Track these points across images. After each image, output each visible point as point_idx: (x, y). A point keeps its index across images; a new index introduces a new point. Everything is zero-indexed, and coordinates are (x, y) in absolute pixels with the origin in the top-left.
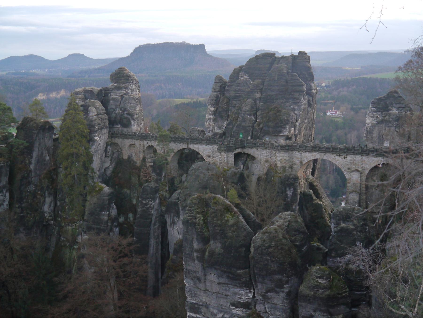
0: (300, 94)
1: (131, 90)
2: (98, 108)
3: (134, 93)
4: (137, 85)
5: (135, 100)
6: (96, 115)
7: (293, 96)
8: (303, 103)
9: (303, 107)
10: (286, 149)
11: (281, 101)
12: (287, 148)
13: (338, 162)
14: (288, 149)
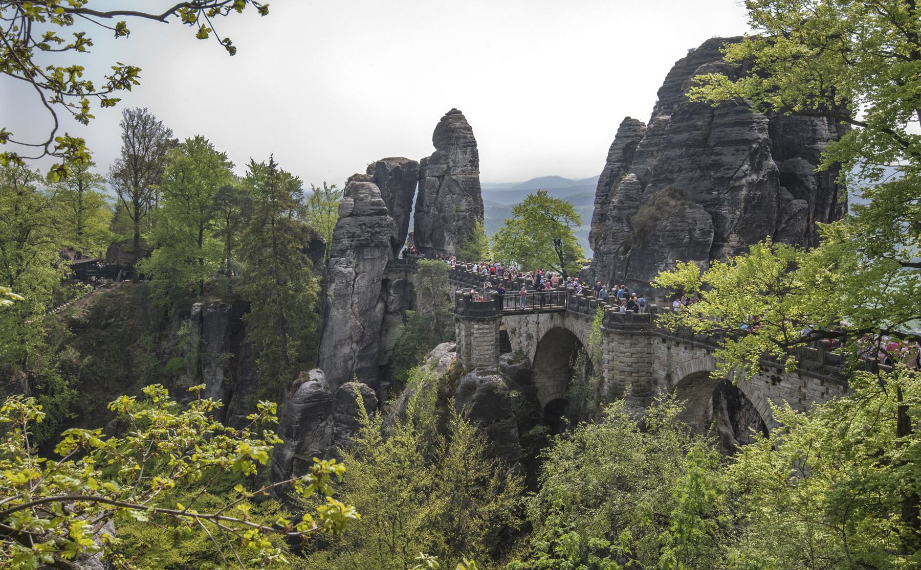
0: (737, 150)
1: (454, 161)
2: (362, 199)
3: (459, 170)
4: (469, 149)
5: (458, 185)
6: (351, 215)
7: (717, 158)
8: (744, 181)
9: (744, 192)
10: (623, 328)
11: (691, 174)
12: (627, 323)
13: (756, 393)
14: (633, 328)
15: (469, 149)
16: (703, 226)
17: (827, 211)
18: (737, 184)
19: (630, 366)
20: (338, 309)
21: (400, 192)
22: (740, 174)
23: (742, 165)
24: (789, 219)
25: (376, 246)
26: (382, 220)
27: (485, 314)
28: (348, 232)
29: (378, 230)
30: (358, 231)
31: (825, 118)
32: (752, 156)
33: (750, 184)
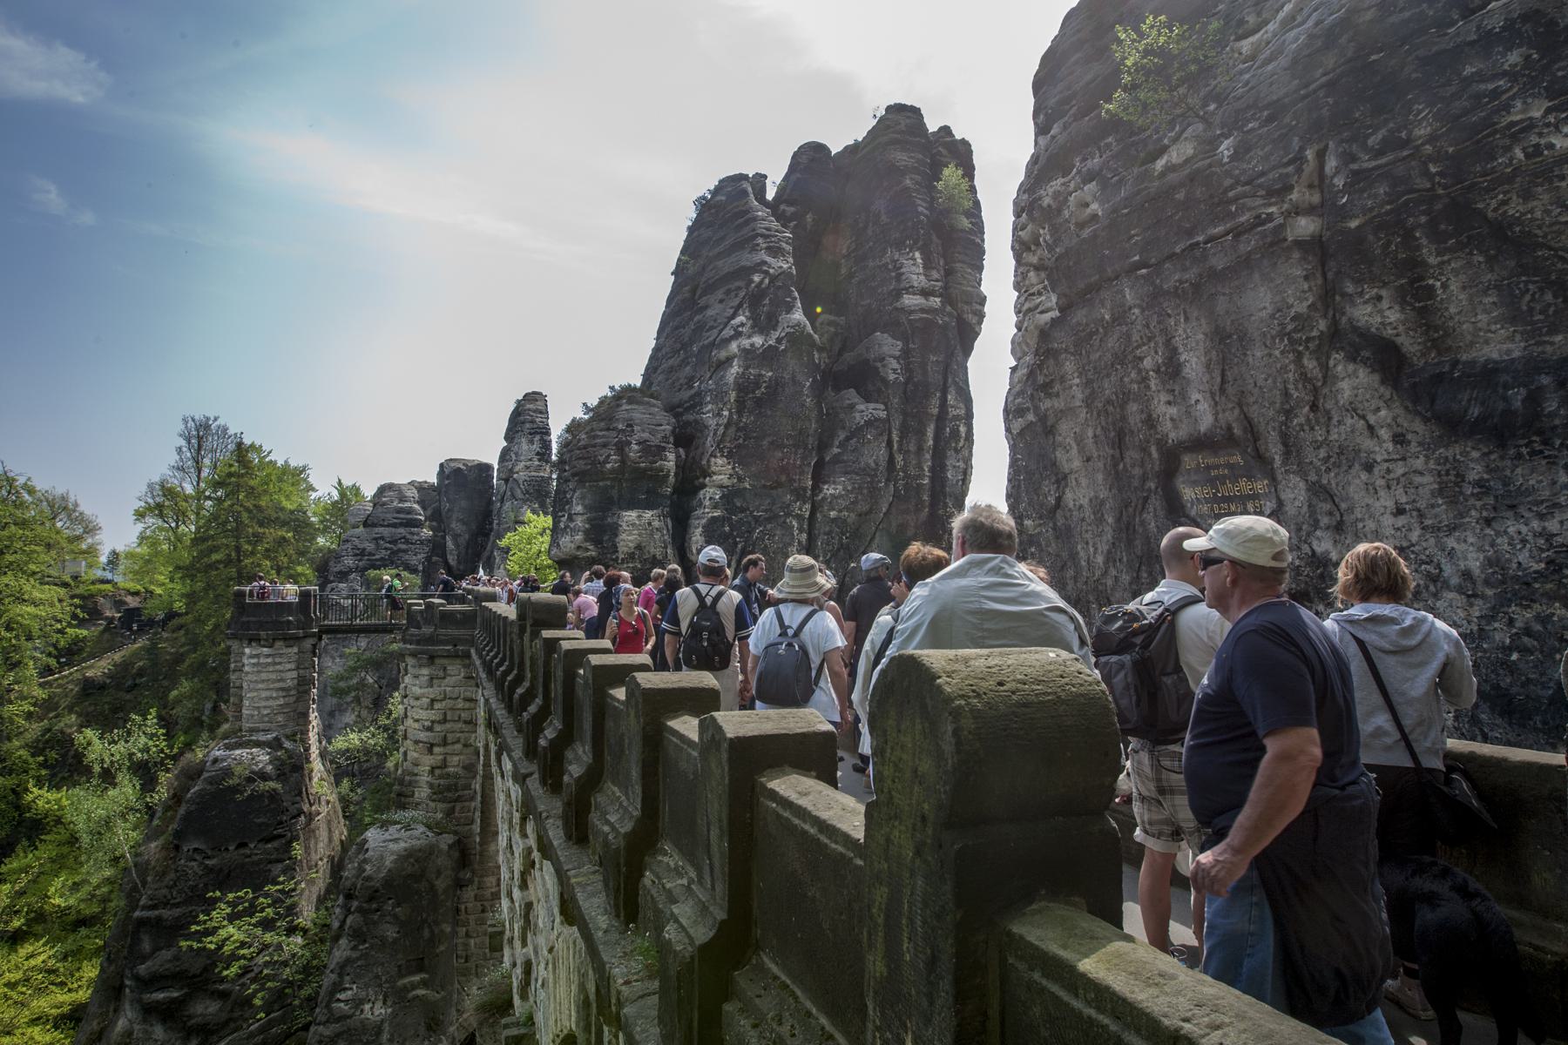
2: (384, 504)
4: (537, 438)
8: (734, 346)
15: (537, 438)
16: (646, 435)
17: (930, 432)
18: (723, 355)
19: (430, 729)
20: (333, 658)
21: (464, 503)
22: (728, 332)
23: (733, 317)
24: (848, 439)
27: (261, 626)
29: (404, 547)
30: (370, 547)
31: (917, 255)
32: (755, 299)
33: (747, 353)
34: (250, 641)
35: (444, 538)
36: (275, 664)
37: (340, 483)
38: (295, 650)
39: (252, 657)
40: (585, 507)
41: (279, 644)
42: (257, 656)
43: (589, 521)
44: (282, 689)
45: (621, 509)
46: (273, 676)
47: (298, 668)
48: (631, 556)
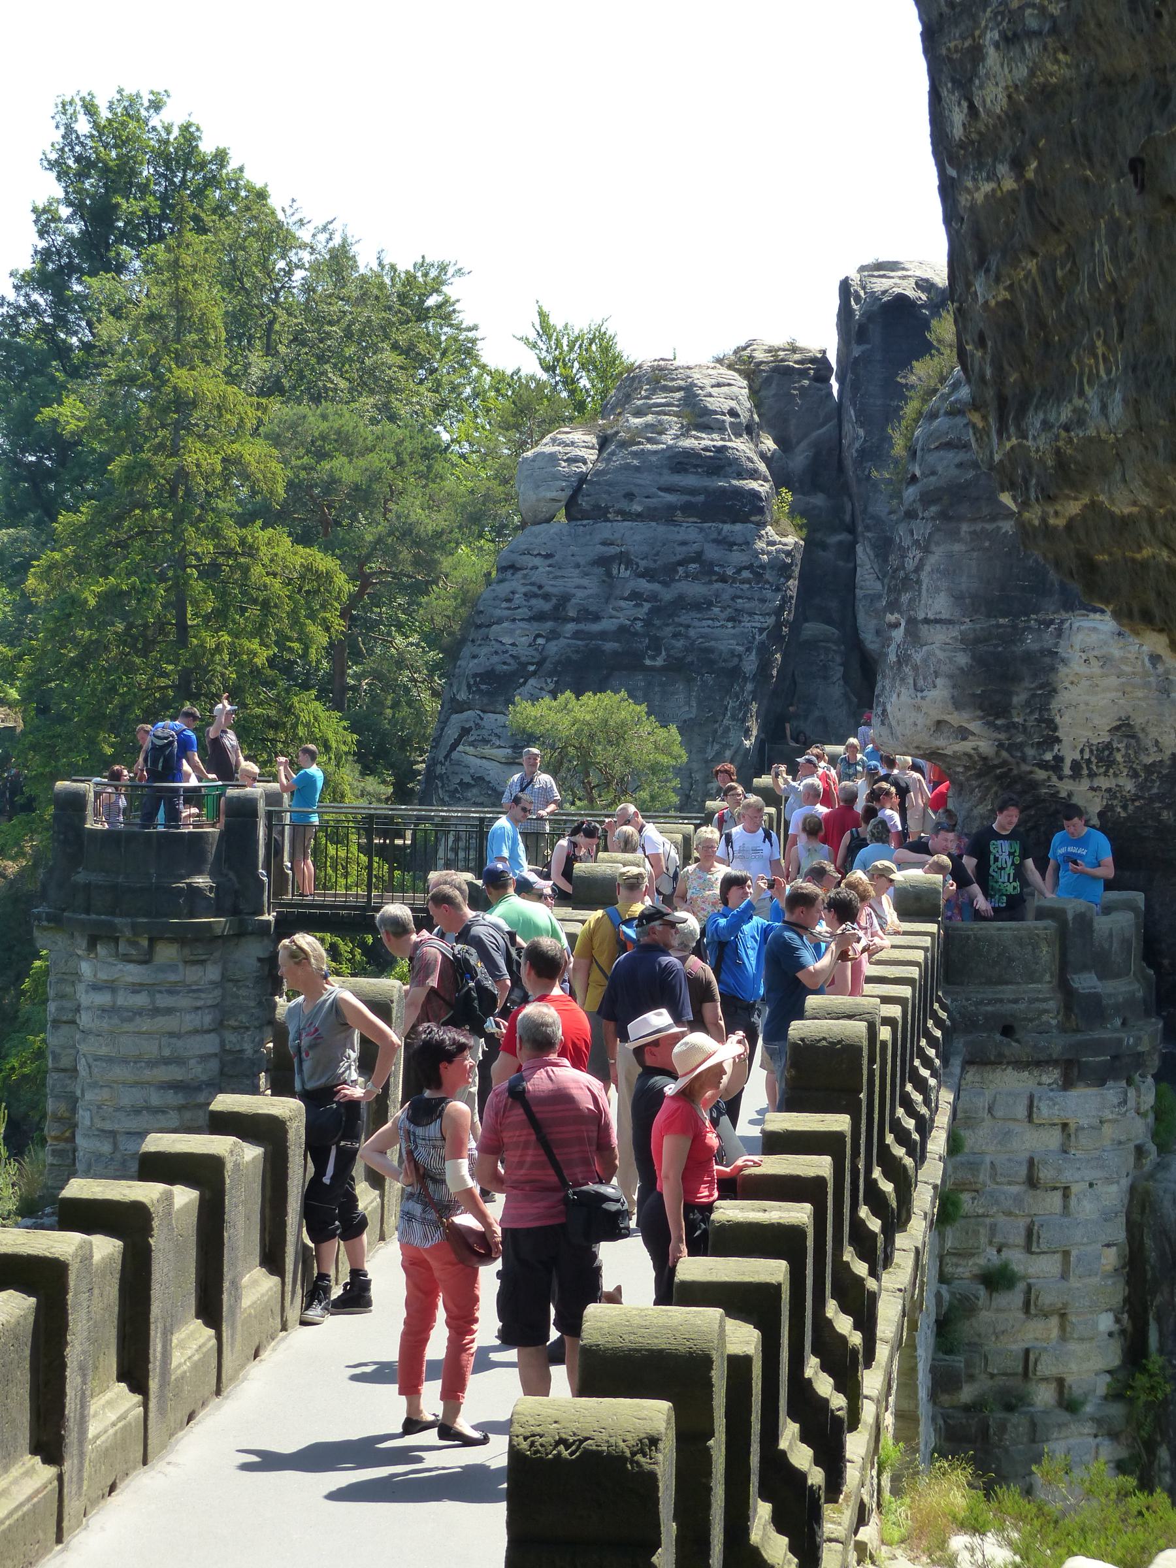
25: (677, 668)
26: (727, 544)
28: (537, 592)
29: (696, 590)
30: (582, 587)
34: (92, 945)
35: (849, 551)
36: (156, 1012)
37: (545, 328)
38: (213, 973)
39: (95, 987)
40: (958, 598)
41: (166, 952)
42: (110, 987)
43: (970, 643)
44: (176, 1086)
45: (1069, 604)
46: (151, 1049)
47: (219, 1027)
48: (1104, 756)
